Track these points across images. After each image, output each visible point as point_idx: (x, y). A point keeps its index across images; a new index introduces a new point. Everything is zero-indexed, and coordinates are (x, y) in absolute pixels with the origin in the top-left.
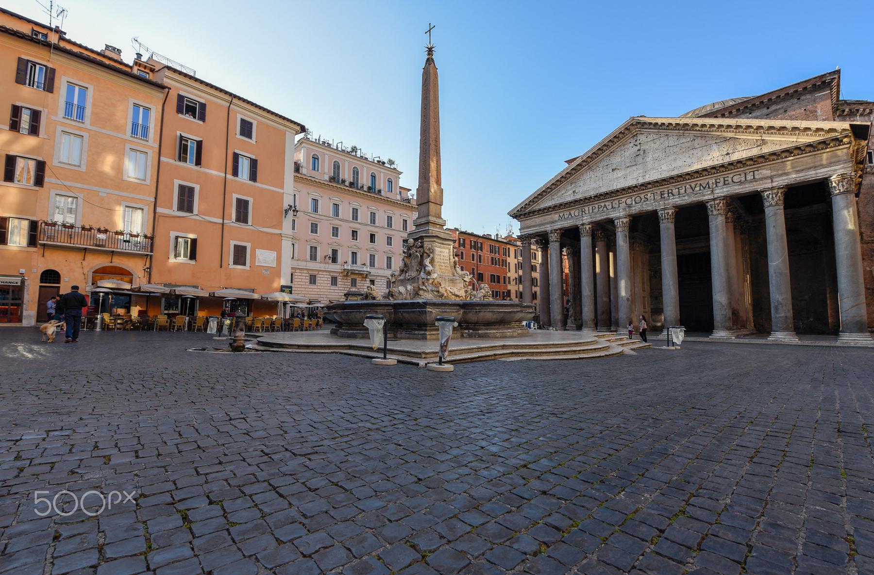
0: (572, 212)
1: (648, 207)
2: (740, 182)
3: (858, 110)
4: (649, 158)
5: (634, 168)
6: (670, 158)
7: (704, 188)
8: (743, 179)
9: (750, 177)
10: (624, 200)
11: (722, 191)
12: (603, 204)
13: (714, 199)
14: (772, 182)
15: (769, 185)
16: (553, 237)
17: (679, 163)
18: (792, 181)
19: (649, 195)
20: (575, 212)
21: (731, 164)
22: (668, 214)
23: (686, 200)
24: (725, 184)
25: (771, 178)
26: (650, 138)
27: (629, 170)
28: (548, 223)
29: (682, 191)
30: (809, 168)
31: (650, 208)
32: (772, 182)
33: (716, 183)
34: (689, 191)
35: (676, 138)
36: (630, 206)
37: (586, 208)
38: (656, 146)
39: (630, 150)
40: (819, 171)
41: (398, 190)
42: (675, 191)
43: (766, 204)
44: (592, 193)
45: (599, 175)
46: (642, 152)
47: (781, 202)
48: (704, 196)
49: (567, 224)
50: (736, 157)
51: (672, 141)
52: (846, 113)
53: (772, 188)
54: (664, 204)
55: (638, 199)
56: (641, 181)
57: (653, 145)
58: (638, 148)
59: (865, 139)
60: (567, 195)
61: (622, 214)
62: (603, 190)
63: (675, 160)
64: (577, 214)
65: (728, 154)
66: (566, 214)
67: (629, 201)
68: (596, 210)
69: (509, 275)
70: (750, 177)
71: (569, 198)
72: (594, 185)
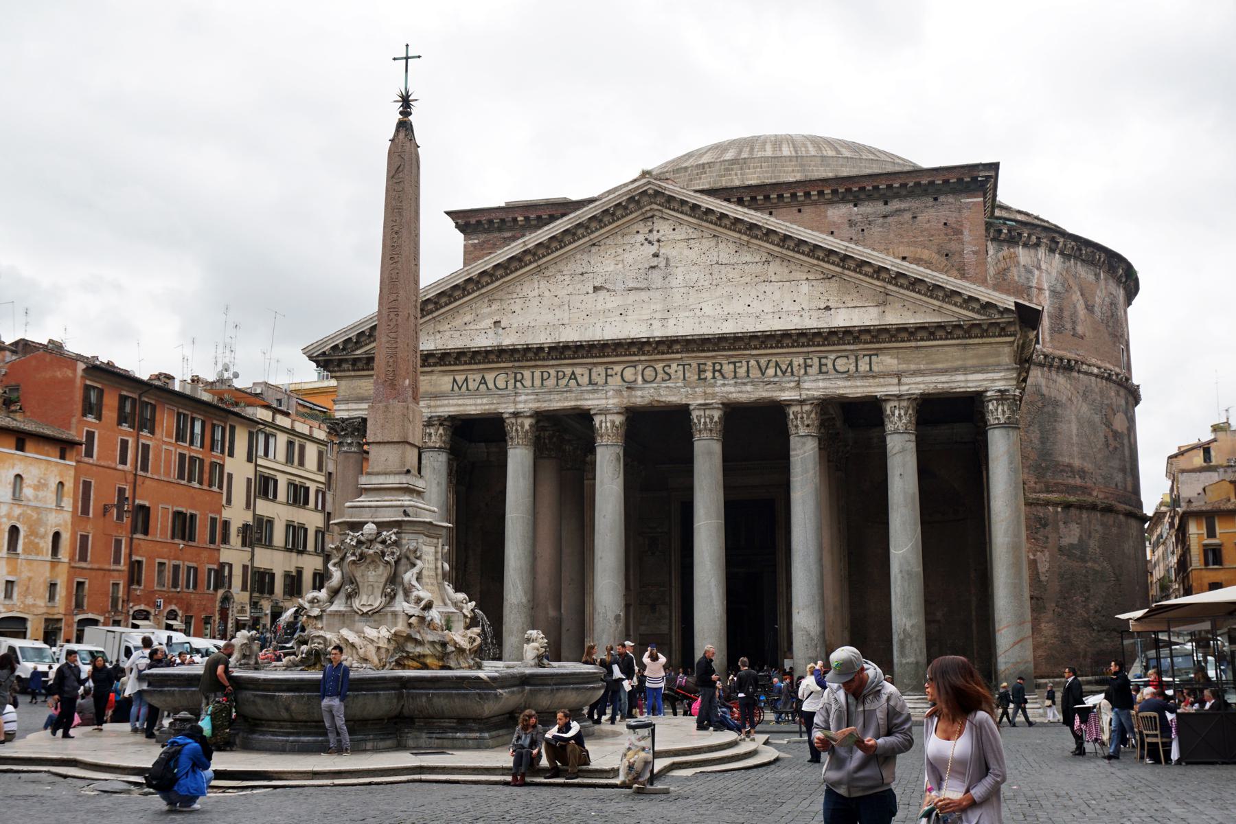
0: (490, 377)
2: (848, 375)
4: (678, 279)
6: (720, 291)
7: (784, 373)
8: (852, 368)
9: (864, 366)
10: (618, 368)
11: (817, 387)
13: (802, 402)
14: (899, 384)
15: (894, 390)
17: (738, 306)
18: (930, 388)
19: (674, 366)
20: (497, 378)
21: (833, 333)
22: (712, 418)
23: (748, 393)
24: (821, 372)
25: (899, 375)
26: (682, 233)
27: (633, 296)
29: (742, 371)
30: (956, 370)
31: (674, 399)
32: (899, 384)
34: (755, 373)
35: (733, 247)
37: (527, 373)
38: (693, 255)
40: (971, 377)
42: (727, 369)
43: (889, 427)
45: (562, 293)
46: (662, 265)
47: (912, 428)
48: (783, 390)
49: (473, 406)
50: (842, 319)
51: (725, 252)
53: (899, 397)
54: (702, 393)
55: (649, 372)
56: (658, 332)
57: (686, 252)
60: (475, 329)
62: (570, 335)
64: (501, 384)
65: (828, 308)
66: (474, 379)
68: (551, 382)
70: (864, 366)
72: (549, 317)
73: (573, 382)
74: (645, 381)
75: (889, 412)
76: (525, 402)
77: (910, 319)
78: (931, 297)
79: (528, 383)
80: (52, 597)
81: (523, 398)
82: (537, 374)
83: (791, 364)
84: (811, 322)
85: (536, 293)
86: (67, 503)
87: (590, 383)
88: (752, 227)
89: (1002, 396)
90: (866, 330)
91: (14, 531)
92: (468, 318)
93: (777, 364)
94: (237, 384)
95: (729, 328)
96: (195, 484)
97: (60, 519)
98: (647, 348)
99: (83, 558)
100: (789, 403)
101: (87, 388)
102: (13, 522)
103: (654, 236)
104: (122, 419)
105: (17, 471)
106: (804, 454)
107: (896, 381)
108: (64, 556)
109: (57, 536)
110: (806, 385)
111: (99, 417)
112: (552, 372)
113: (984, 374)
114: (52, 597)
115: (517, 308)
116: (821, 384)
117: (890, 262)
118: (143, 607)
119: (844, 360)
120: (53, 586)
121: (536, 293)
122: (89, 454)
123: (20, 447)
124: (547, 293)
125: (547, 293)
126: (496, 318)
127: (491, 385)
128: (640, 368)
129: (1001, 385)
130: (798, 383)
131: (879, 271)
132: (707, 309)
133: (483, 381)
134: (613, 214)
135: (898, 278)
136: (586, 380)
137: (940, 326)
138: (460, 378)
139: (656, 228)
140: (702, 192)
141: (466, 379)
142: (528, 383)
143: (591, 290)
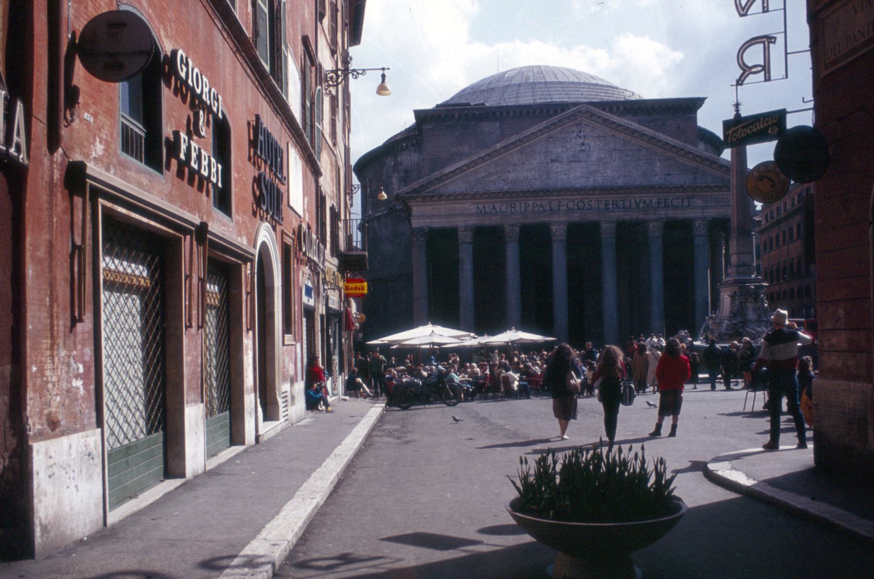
0: (497, 206)
1: (591, 217)
5: (578, 165)
10: (565, 202)
12: (539, 203)
13: (657, 220)
15: (700, 215)
28: (462, 215)
29: (627, 205)
33: (659, 203)
34: (634, 206)
36: (570, 211)
42: (620, 204)
53: (703, 219)
58: (581, 141)
61: (562, 219)
67: (571, 205)
70: (686, 204)
71: (498, 184)
73: (541, 209)
74: (579, 209)
75: (697, 225)
82: (523, 204)
93: (644, 202)
103: (582, 134)
115: (510, 169)
119: (676, 201)
128: (576, 202)
139: (583, 129)
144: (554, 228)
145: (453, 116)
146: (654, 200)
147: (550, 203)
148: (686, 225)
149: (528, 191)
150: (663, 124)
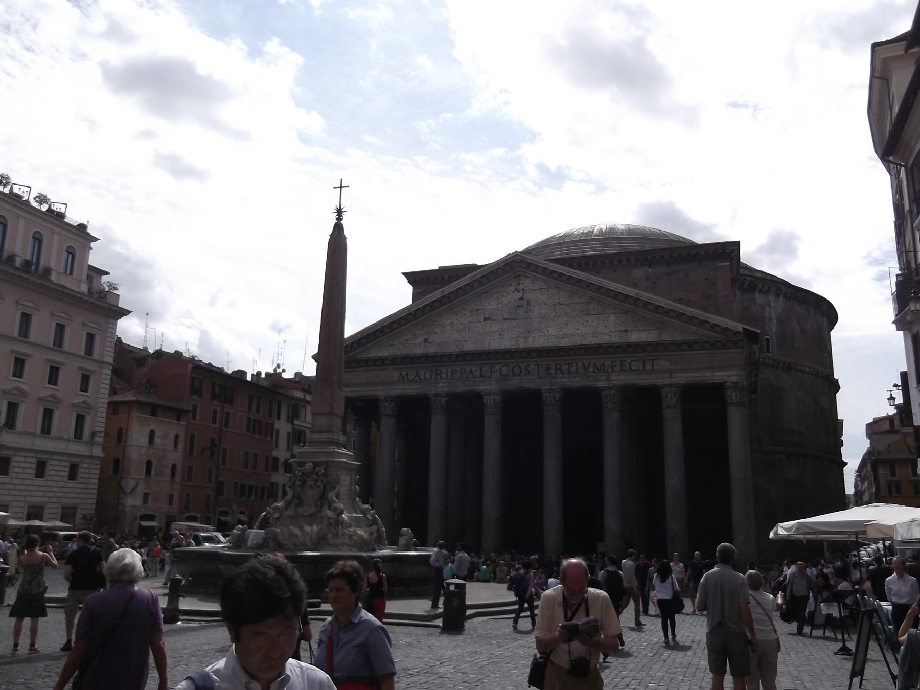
0: (421, 373)
1: (530, 383)
3: (757, 286)
5: (514, 323)
7: (599, 370)
8: (641, 367)
9: (648, 366)
10: (498, 367)
11: (619, 379)
12: (468, 368)
13: (610, 388)
14: (671, 377)
16: (387, 409)
19: (532, 366)
23: (576, 382)
24: (622, 370)
29: (573, 369)
31: (531, 386)
33: (613, 366)
39: (510, 297)
41: (85, 271)
42: (565, 368)
44: (453, 349)
46: (525, 304)
49: (412, 389)
52: (745, 286)
53: (670, 386)
54: (551, 383)
55: (516, 370)
56: (522, 345)
58: (520, 295)
59: (757, 344)
61: (494, 387)
62: (470, 347)
63: (566, 324)
64: (428, 376)
65: (626, 331)
67: (505, 370)
69: (275, 454)
71: (418, 350)
76: (442, 387)
77: (678, 338)
78: (690, 324)
79: (444, 376)
80: (171, 503)
81: (441, 385)
82: (450, 371)
83: (603, 365)
84: (615, 339)
85: (449, 322)
86: (181, 447)
87: (481, 376)
88: (579, 281)
89: (735, 386)
90: (649, 344)
91: (149, 464)
92: (409, 337)
94: (286, 376)
95: (565, 342)
96: (257, 436)
97: (176, 456)
98: (515, 355)
99: (189, 479)
100: (603, 389)
101: (193, 379)
102: (149, 458)
104: (214, 397)
105: (152, 427)
106: (612, 420)
107: (668, 375)
108: (178, 479)
109: (174, 467)
110: (613, 378)
111: (200, 396)
112: (458, 369)
113: (727, 373)
114: (171, 503)
116: (622, 377)
117: (664, 302)
118: (224, 509)
120: (171, 496)
121: (449, 322)
122: (194, 417)
123: (154, 413)
124: (456, 322)
125: (456, 322)
126: (426, 337)
127: (422, 377)
128: (511, 367)
129: (734, 379)
130: (608, 376)
131: (658, 308)
132: (552, 331)
133: (417, 375)
134: (496, 274)
135: (668, 312)
136: (478, 374)
137: (695, 342)
138: (404, 373)
140: (552, 261)
141: (407, 374)
142: (444, 376)
143: (482, 320)
144: (485, 398)
145: (443, 278)
146: (608, 363)
147: (481, 369)
148: (652, 394)
149: (451, 355)
150: (687, 275)
